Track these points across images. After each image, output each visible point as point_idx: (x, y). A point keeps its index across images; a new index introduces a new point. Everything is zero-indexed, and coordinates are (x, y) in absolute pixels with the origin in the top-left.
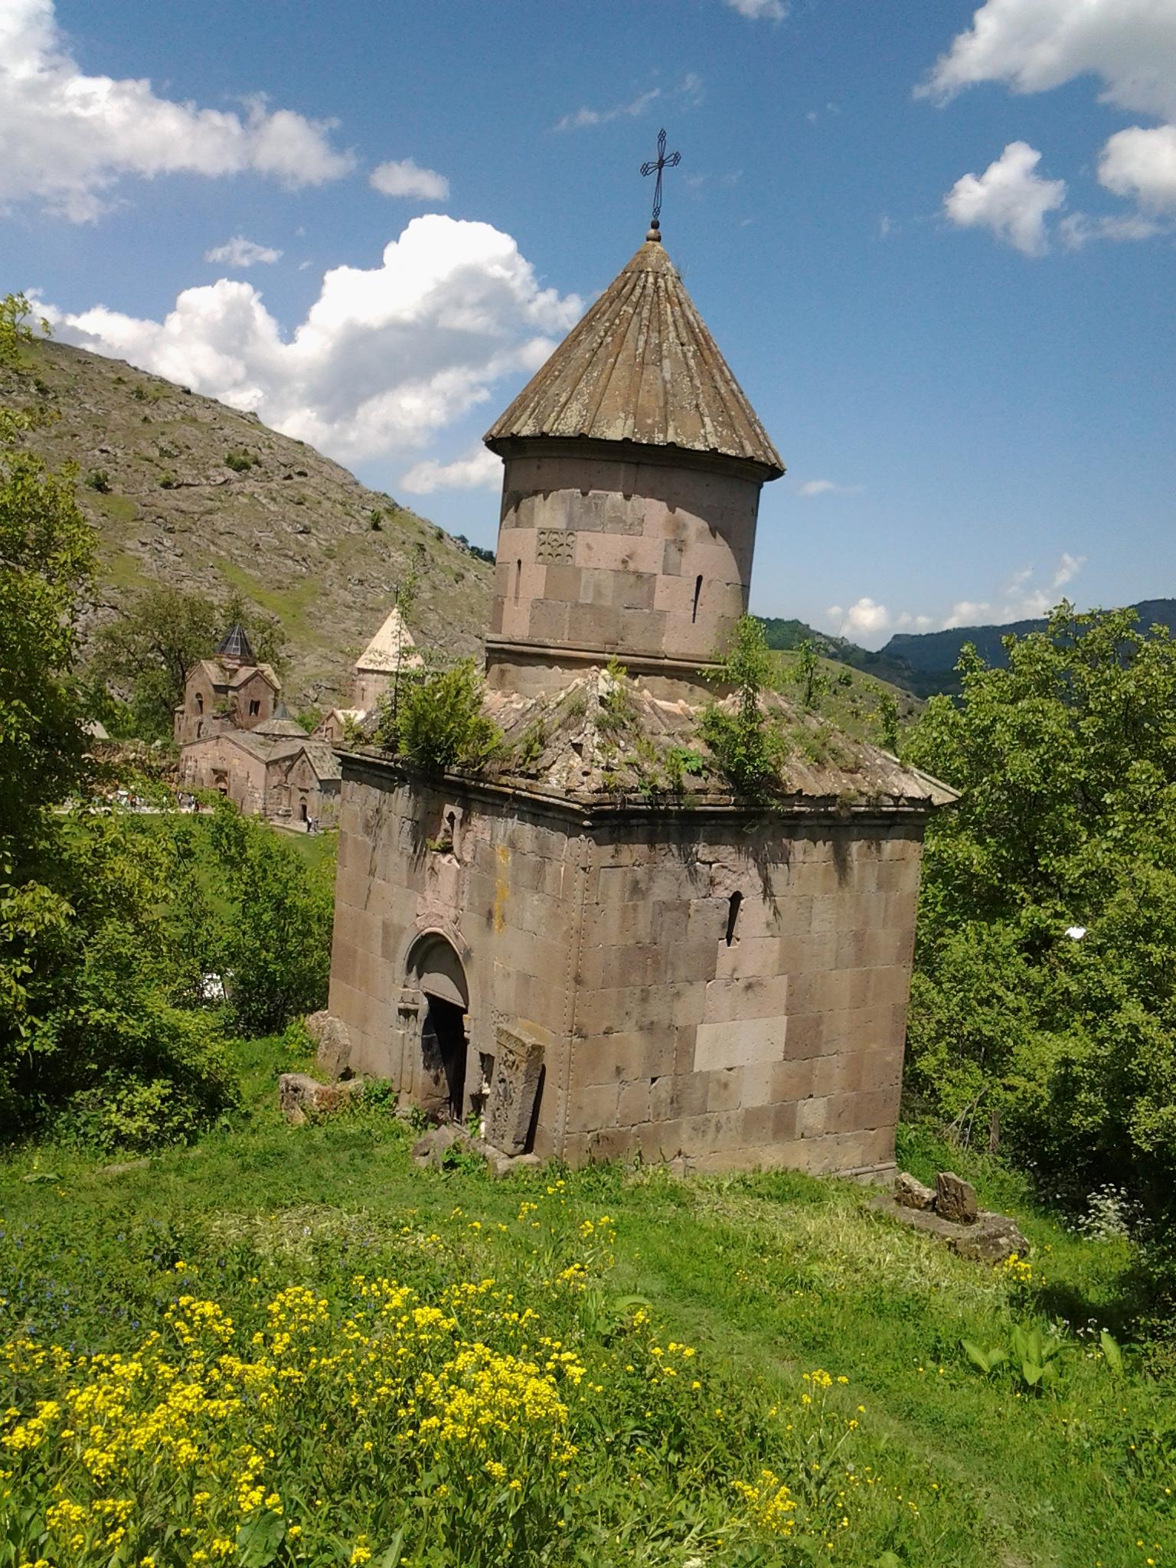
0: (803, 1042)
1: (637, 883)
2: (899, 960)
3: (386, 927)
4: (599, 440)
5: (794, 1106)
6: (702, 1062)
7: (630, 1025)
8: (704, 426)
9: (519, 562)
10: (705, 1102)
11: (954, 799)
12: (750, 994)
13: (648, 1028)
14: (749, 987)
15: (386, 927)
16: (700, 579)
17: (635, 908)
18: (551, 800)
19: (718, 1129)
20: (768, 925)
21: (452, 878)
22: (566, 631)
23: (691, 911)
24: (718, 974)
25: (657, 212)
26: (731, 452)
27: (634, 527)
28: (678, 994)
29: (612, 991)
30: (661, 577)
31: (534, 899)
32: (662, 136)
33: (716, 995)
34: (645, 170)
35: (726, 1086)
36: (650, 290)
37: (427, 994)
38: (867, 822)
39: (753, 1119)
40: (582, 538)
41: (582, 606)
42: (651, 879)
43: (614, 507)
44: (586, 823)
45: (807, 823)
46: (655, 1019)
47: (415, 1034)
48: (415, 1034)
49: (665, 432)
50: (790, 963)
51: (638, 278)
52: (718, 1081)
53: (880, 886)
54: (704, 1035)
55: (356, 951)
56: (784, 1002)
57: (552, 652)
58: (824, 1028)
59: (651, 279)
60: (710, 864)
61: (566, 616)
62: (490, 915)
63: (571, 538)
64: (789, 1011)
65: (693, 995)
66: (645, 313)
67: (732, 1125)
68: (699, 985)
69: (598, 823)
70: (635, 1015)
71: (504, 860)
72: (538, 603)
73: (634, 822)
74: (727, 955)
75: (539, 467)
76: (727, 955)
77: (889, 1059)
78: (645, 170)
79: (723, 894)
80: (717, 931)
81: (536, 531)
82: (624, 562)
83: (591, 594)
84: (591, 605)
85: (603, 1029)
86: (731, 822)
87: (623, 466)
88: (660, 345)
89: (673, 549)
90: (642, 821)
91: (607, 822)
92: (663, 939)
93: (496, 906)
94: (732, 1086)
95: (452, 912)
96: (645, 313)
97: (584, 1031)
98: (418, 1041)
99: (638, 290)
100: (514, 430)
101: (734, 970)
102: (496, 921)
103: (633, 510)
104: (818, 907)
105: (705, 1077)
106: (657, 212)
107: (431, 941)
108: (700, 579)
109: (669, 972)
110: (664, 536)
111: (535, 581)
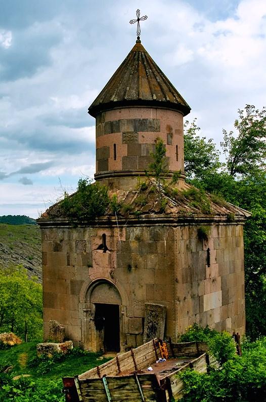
2: (242, 270)
3: (72, 282)
5: (225, 321)
8: (175, 96)
9: (115, 145)
11: (250, 215)
13: (193, 297)
14: (213, 281)
15: (72, 282)
18: (159, 219)
21: (107, 258)
22: (138, 166)
25: (139, 34)
27: (157, 129)
28: (199, 285)
31: (153, 256)
32: (138, 11)
33: (207, 284)
35: (211, 316)
36: (144, 57)
37: (95, 304)
40: (140, 134)
41: (143, 157)
43: (150, 123)
44: (176, 224)
45: (222, 224)
47: (91, 319)
48: (91, 319)
49: (166, 98)
50: (221, 271)
51: (139, 54)
54: (205, 297)
55: (57, 295)
56: (220, 286)
57: (133, 173)
58: (229, 294)
61: (137, 161)
62: (129, 267)
63: (136, 134)
66: (145, 63)
70: (190, 293)
71: (134, 245)
72: (124, 158)
75: (120, 112)
76: (208, 269)
78: (131, 22)
79: (205, 249)
80: (205, 262)
81: (121, 133)
82: (155, 141)
83: (145, 152)
84: (146, 156)
87: (152, 109)
88: (153, 73)
89: (169, 136)
93: (132, 263)
95: (109, 270)
96: (145, 63)
98: (92, 323)
100: (112, 99)
101: (210, 275)
102: (133, 268)
103: (156, 123)
106: (139, 34)
110: (166, 132)
111: (123, 150)
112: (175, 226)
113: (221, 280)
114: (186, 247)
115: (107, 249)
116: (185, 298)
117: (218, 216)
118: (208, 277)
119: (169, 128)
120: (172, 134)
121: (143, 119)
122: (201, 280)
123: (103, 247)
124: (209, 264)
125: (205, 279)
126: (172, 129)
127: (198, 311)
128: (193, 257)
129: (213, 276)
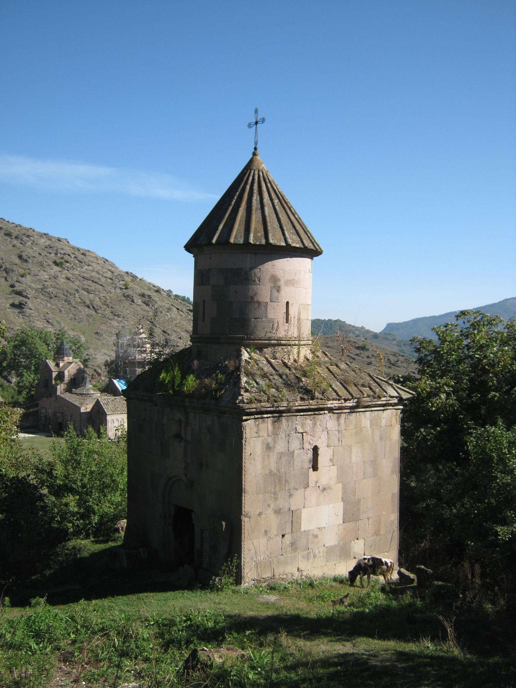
0: (351, 514)
1: (268, 444)
2: (393, 473)
4: (238, 244)
6: (304, 527)
7: (270, 511)
8: (284, 234)
9: (204, 301)
10: (308, 544)
11: (410, 396)
12: (325, 493)
13: (278, 512)
14: (324, 489)
16: (287, 303)
17: (268, 456)
19: (315, 556)
20: (331, 460)
23: (295, 454)
24: (310, 485)
25: (256, 143)
26: (298, 246)
28: (291, 495)
29: (261, 496)
30: (269, 303)
32: (256, 111)
34: (250, 126)
35: (316, 536)
38: (373, 409)
39: (330, 551)
42: (275, 442)
46: (281, 507)
50: (341, 477)
51: (250, 173)
52: (313, 535)
53: (381, 439)
54: (305, 513)
59: (256, 173)
60: (302, 433)
64: (343, 500)
65: (298, 495)
67: (321, 555)
68: (301, 491)
69: (248, 417)
70: (272, 506)
73: (265, 416)
74: (313, 475)
75: (210, 258)
77: (392, 519)
78: (250, 126)
79: (309, 447)
85: (258, 513)
86: (310, 413)
89: (275, 291)
90: (269, 415)
91: (253, 417)
92: (283, 470)
94: (320, 537)
97: (249, 515)
99: (251, 178)
101: (317, 482)
104: (354, 450)
105: (307, 532)
106: (256, 143)
107: (174, 479)
108: (287, 303)
109: (287, 485)
112: (246, 420)
113: (343, 488)
114: (265, 446)
115: (182, 439)
116: (260, 514)
117: (337, 402)
118: (312, 483)
119: (275, 280)
120: (279, 287)
121: (237, 269)
122: (297, 489)
123: (178, 436)
124: (315, 468)
125: (307, 486)
126: (279, 280)
127: (288, 530)
128: (281, 458)
129: (324, 482)
